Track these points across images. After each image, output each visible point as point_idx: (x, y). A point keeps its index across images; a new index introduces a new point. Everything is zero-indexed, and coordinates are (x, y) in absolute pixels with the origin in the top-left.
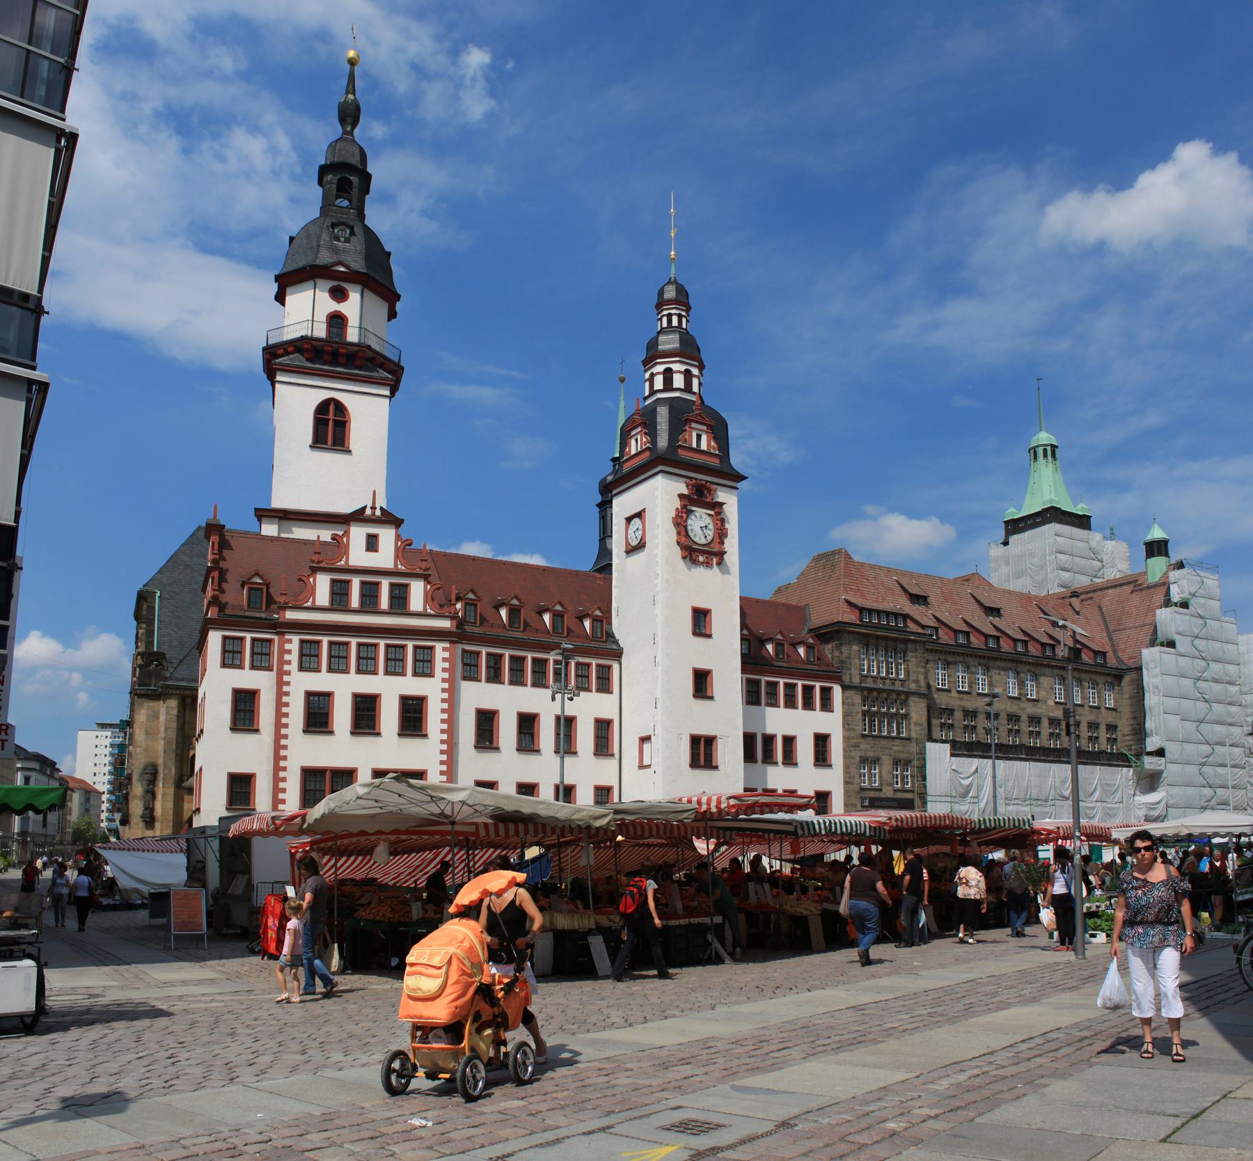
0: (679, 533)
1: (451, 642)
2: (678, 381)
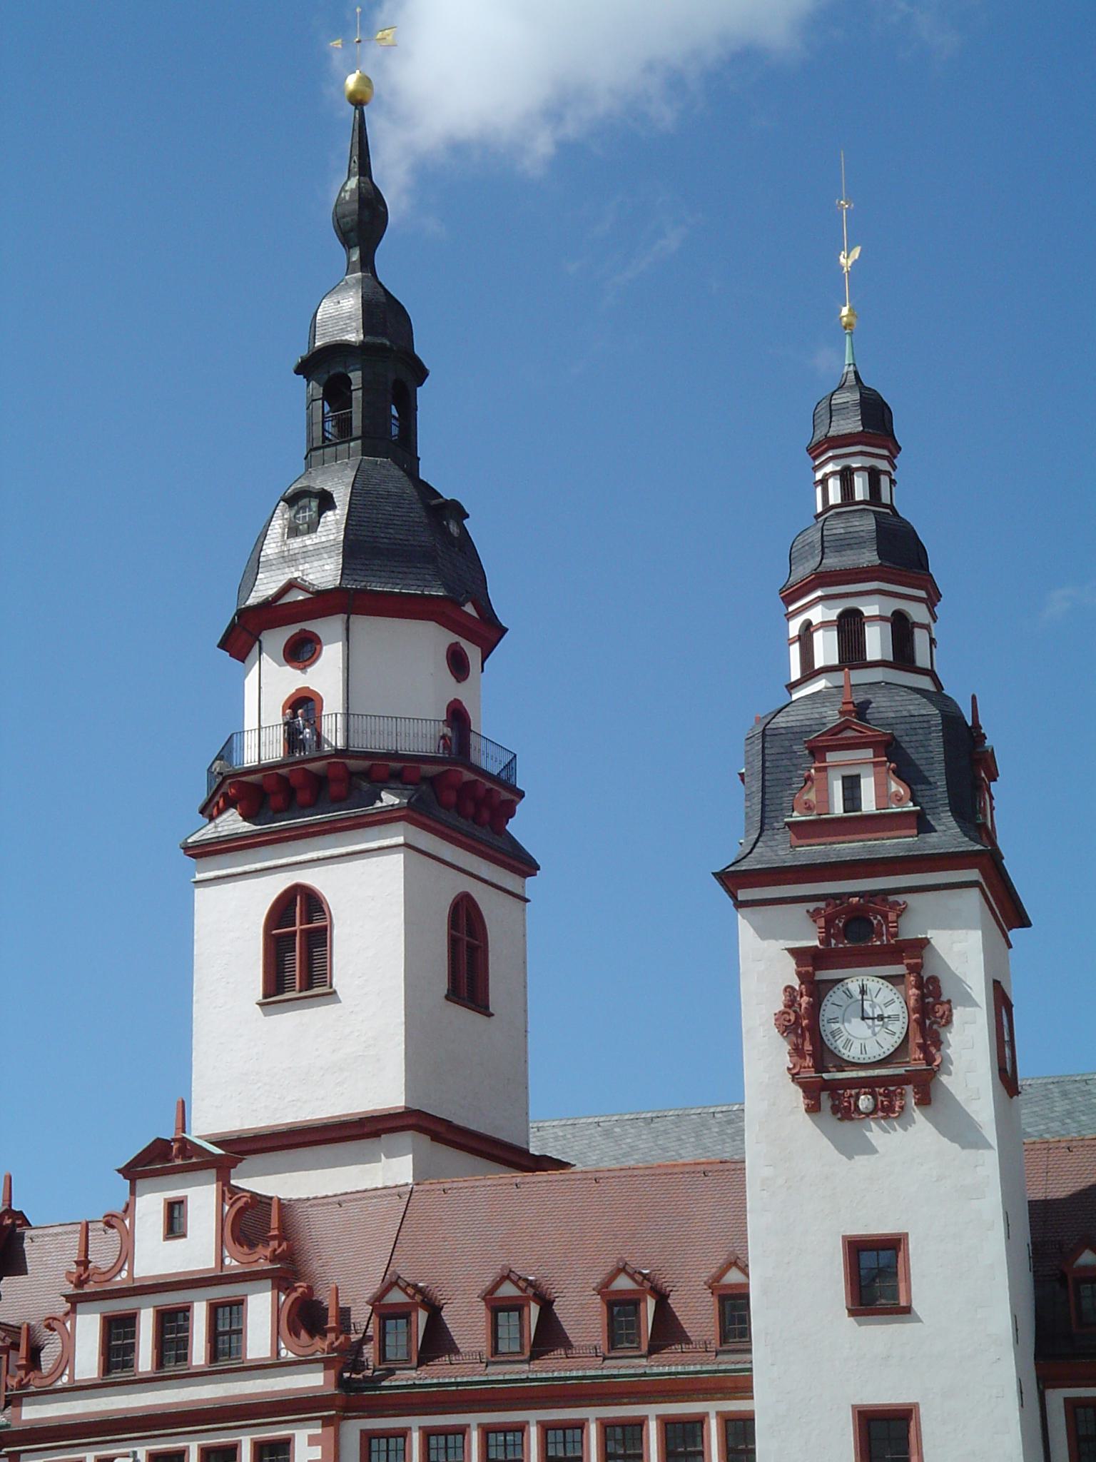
0: (797, 1051)
1: (326, 1422)
2: (876, 643)
